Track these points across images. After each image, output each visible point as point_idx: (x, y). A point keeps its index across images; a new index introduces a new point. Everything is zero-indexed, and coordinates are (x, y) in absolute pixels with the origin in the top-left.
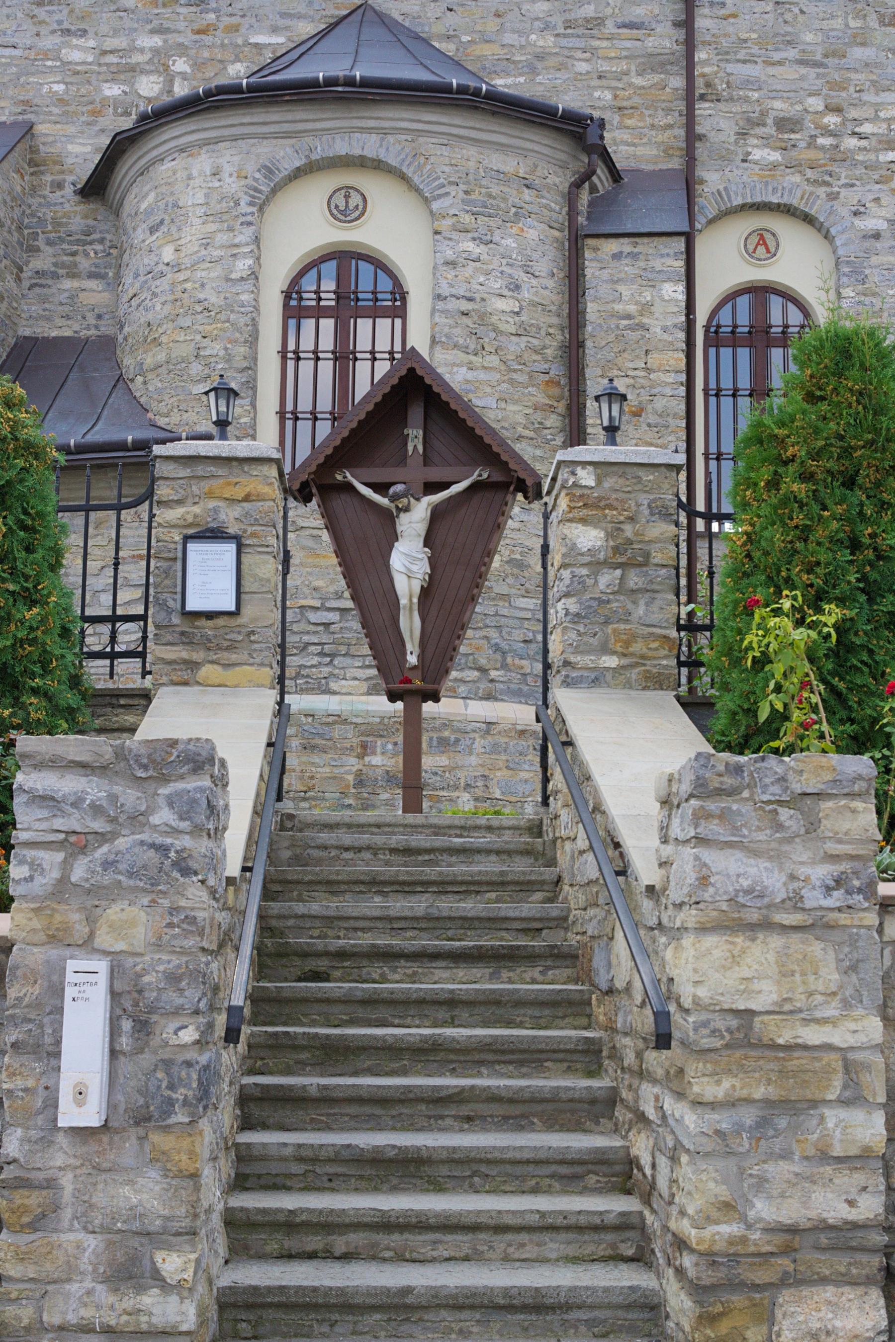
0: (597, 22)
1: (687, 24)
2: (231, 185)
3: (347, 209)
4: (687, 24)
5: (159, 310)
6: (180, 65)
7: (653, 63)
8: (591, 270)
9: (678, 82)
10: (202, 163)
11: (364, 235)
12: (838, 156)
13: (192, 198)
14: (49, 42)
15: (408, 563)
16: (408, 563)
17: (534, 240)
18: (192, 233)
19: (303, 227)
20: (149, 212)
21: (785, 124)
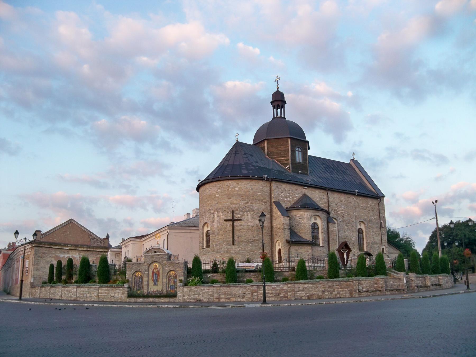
3: (315, 219)
7: (326, 203)
9: (327, 205)
10: (306, 213)
11: (317, 222)
12: (338, 214)
13: (305, 217)
14: (280, 193)
15: (345, 256)
16: (345, 256)
17: (326, 222)
19: (313, 221)
21: (335, 210)
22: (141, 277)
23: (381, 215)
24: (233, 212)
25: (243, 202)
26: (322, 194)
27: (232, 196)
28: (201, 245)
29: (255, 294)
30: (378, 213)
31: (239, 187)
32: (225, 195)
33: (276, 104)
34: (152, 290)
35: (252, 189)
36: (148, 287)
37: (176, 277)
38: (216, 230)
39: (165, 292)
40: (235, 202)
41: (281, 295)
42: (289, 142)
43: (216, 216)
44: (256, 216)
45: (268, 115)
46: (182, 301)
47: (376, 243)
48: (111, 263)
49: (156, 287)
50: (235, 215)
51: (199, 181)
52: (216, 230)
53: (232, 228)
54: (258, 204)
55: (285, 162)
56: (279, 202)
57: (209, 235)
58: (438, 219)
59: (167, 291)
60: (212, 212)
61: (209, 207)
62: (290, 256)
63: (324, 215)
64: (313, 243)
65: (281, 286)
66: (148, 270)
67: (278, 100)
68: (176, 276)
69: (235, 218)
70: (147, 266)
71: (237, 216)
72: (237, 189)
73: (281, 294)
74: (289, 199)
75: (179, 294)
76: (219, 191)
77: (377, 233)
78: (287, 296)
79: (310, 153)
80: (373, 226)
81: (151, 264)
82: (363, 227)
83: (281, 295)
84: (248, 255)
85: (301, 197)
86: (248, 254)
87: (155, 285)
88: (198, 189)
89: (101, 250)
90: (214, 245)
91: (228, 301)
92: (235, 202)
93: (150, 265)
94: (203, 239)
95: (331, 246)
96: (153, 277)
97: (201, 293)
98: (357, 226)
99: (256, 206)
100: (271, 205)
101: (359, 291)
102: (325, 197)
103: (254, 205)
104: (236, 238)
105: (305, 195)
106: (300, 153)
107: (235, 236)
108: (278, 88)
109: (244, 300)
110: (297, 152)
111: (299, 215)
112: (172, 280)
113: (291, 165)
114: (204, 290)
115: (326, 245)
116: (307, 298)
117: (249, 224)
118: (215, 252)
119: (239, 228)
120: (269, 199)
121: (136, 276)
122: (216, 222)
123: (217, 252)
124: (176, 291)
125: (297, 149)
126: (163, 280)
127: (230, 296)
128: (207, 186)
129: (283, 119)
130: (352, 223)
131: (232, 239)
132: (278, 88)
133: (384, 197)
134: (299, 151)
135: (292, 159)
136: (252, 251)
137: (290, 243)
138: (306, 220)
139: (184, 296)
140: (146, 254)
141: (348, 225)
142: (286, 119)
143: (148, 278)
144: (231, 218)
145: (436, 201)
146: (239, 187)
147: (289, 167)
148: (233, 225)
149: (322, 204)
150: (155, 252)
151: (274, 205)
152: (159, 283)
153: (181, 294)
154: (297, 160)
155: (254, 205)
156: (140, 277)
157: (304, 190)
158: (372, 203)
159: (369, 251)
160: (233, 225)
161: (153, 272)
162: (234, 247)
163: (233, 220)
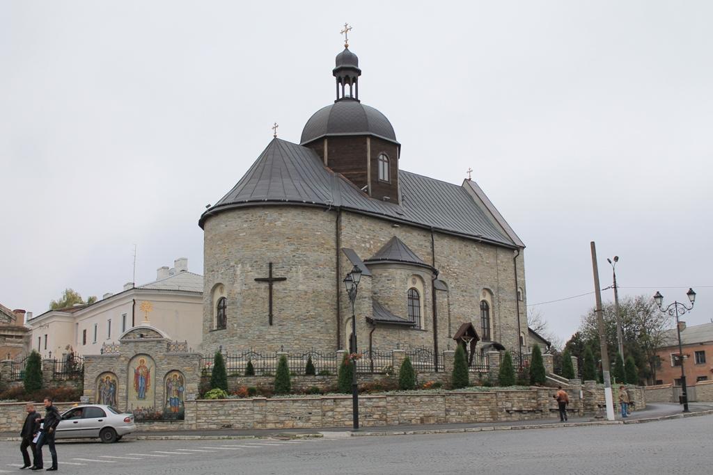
0: (422, 245)
1: (433, 247)
2: (404, 277)
3: (414, 283)
4: (433, 247)
5: (391, 295)
6: (372, 242)
8: (437, 295)
9: (431, 258)
10: (399, 271)
13: (397, 277)
14: (354, 234)
15: (468, 348)
16: (468, 348)
18: (398, 283)
19: (410, 285)
20: (386, 276)
21: (443, 267)
22: (113, 384)
23: (518, 279)
24: (271, 265)
25: (289, 248)
26: (423, 238)
27: (271, 236)
28: (208, 324)
29: (330, 414)
30: (514, 276)
31: (283, 219)
32: (257, 233)
33: (343, 75)
34: (135, 408)
35: (307, 225)
36: (127, 402)
37: (182, 383)
38: (239, 297)
39: (160, 410)
40: (275, 247)
41: (375, 416)
42: (369, 143)
43: (238, 272)
44: (311, 273)
45: (325, 93)
46: (194, 427)
47: (511, 328)
48: (48, 358)
49: (143, 401)
50: (274, 270)
51: (207, 207)
52: (239, 297)
53: (268, 295)
54: (317, 251)
55: (359, 179)
56: (353, 250)
57: (224, 307)
58: (618, 289)
59: (164, 409)
60: (232, 264)
61: (226, 255)
62: (373, 346)
63: (427, 276)
64: (407, 326)
65: (374, 400)
66: (128, 369)
67: (347, 70)
68: (181, 381)
69: (274, 276)
70: (126, 363)
71: (277, 273)
72: (279, 223)
73: (374, 414)
74: (368, 245)
75: (189, 414)
76: (244, 226)
77: (512, 310)
78: (384, 417)
79: (404, 164)
80: (506, 298)
81: (133, 358)
82: (488, 298)
83: (375, 416)
84: (296, 344)
85: (390, 242)
86: (297, 342)
87: (141, 397)
88: (202, 223)
89: (10, 333)
90: (235, 325)
91: (281, 426)
92: (275, 247)
93: (131, 360)
94: (213, 314)
95: (438, 331)
96: (137, 383)
97: (230, 412)
98: (479, 297)
99: (313, 256)
100: (338, 254)
101: (508, 411)
102: (428, 244)
103: (308, 254)
104: (275, 313)
105: (395, 239)
106: (386, 164)
107: (274, 308)
108: (346, 46)
109: (309, 425)
110: (381, 163)
111: (387, 274)
112: (174, 388)
113: (369, 184)
114: (236, 406)
115: (431, 328)
116: (419, 422)
117: (301, 287)
118: (235, 338)
119: (281, 295)
120: (334, 244)
121: (102, 381)
122: (241, 284)
123: (241, 337)
124: (184, 408)
125: (381, 157)
126: (156, 388)
127: (283, 419)
128: (223, 217)
129: (355, 103)
130: (471, 291)
131: (268, 313)
132: (346, 46)
133: (524, 247)
134: (383, 161)
135: (372, 175)
136: (304, 337)
137: (374, 323)
138: (398, 283)
139: (198, 418)
140: (124, 339)
141: (464, 294)
142: (359, 101)
143: (127, 385)
144: (267, 276)
145: (616, 259)
146: (283, 219)
147: (367, 189)
148: (271, 288)
149: (424, 258)
150: (142, 336)
151: (344, 254)
152: (149, 394)
153: (193, 415)
154: (381, 177)
155: (308, 254)
156: (110, 384)
157: (394, 229)
158: (504, 257)
159: (498, 342)
160: (271, 288)
161: (137, 375)
162: (272, 329)
163: (270, 280)
